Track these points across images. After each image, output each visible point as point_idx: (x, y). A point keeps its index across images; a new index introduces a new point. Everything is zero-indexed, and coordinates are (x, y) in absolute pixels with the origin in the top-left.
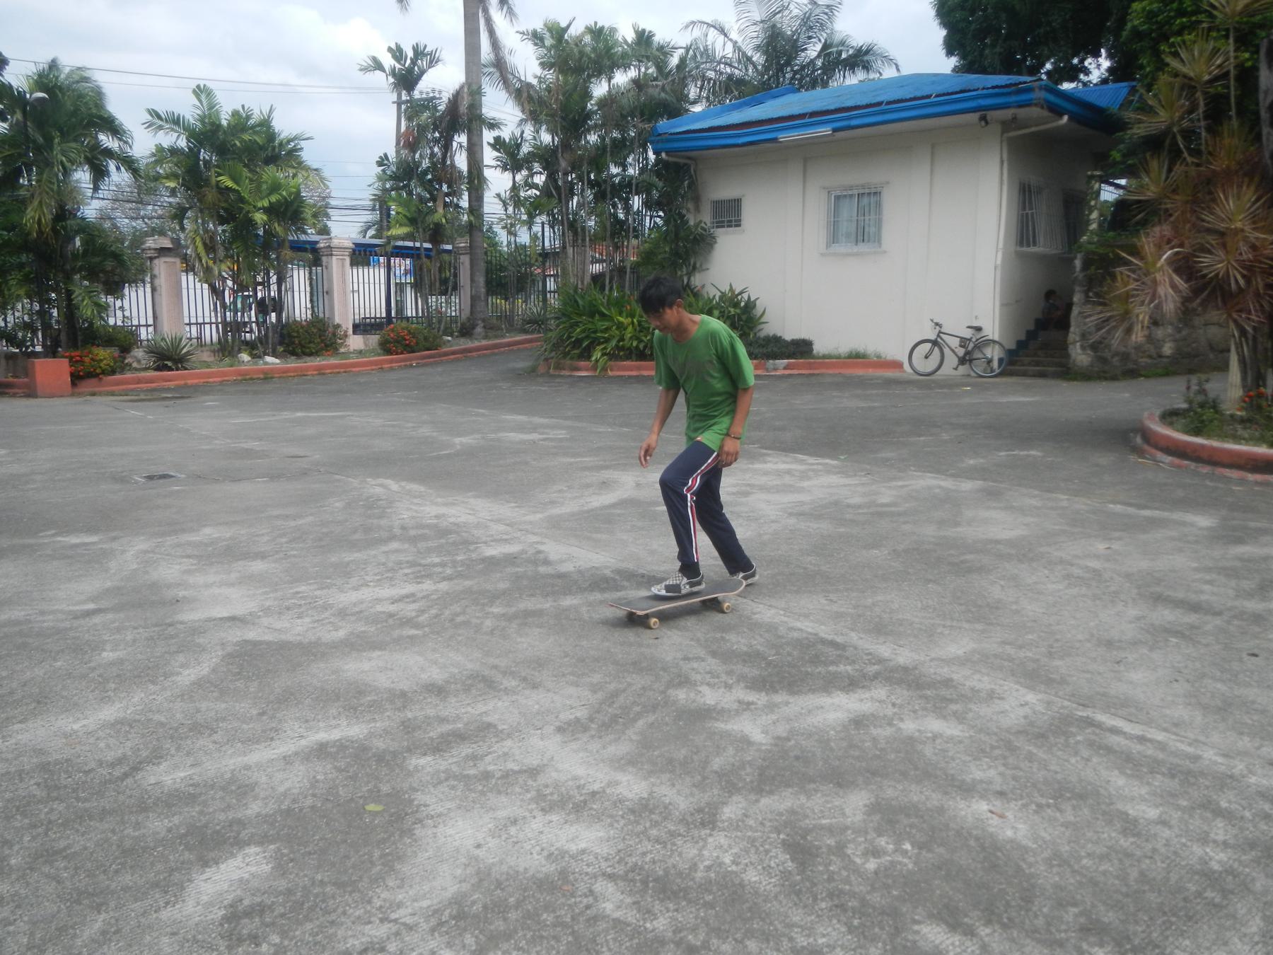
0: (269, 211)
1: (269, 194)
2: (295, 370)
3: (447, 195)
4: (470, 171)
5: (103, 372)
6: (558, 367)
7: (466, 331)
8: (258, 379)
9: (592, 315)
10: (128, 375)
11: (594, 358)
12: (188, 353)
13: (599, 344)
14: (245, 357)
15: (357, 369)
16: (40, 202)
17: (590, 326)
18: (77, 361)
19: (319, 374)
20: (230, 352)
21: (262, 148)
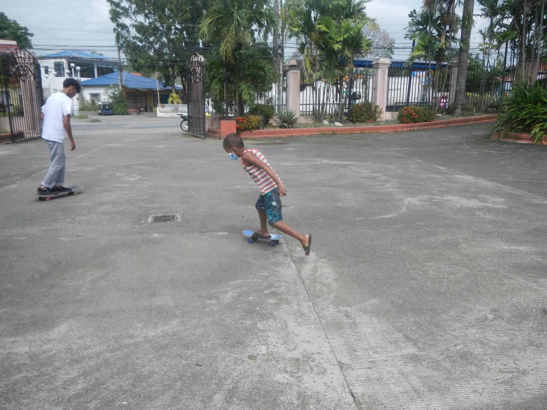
0: (345, 43)
1: (345, 33)
2: (349, 130)
3: (448, 32)
4: (463, 17)
5: (253, 128)
6: (506, 136)
7: (450, 111)
8: (329, 134)
9: (536, 103)
10: (266, 130)
11: (533, 132)
12: (296, 119)
13: (539, 123)
14: (326, 122)
15: (383, 131)
16: (227, 41)
17: (533, 110)
18: (241, 122)
19: (361, 133)
20: (319, 120)
21: (343, 8)
